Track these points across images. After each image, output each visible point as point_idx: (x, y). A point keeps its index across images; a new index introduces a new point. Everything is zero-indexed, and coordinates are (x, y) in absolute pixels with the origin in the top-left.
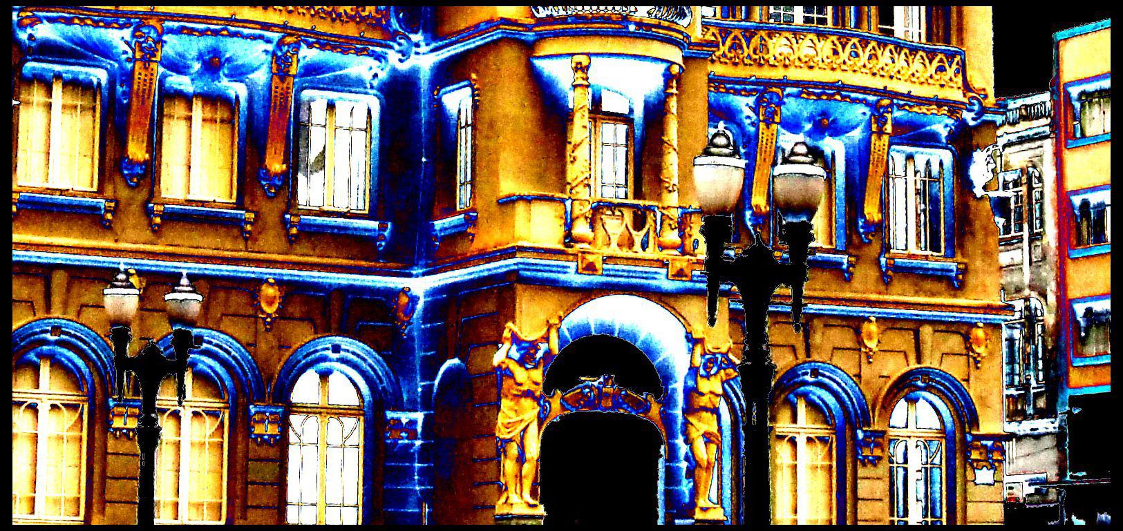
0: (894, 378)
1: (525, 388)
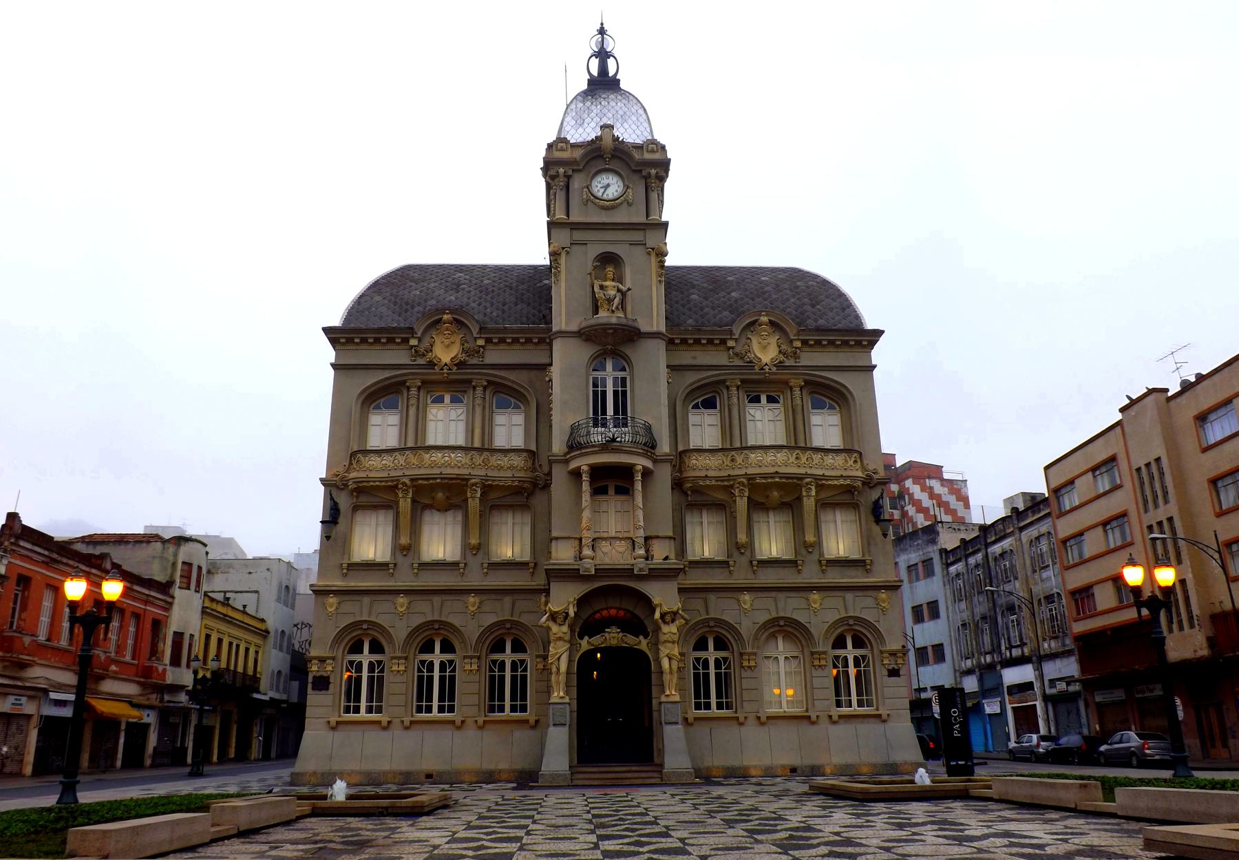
0: (831, 622)
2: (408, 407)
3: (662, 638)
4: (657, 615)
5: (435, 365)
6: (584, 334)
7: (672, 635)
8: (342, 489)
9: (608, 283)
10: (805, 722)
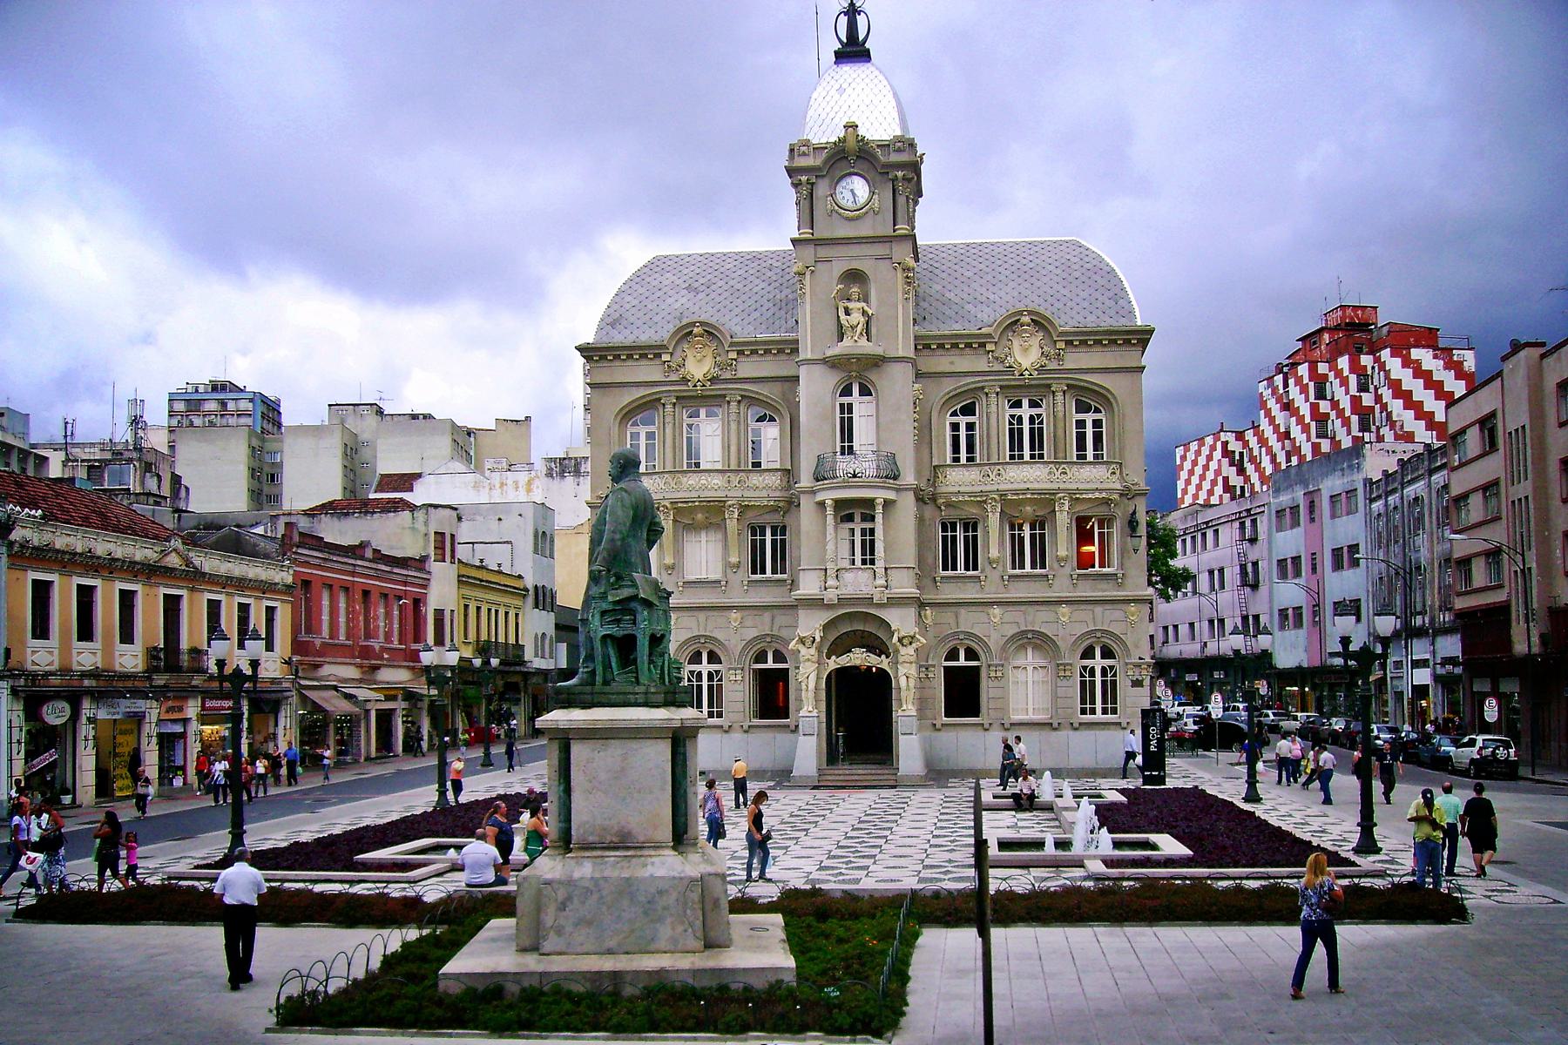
3: (901, 659)
4: (895, 639)
9: (851, 305)
10: (1047, 727)
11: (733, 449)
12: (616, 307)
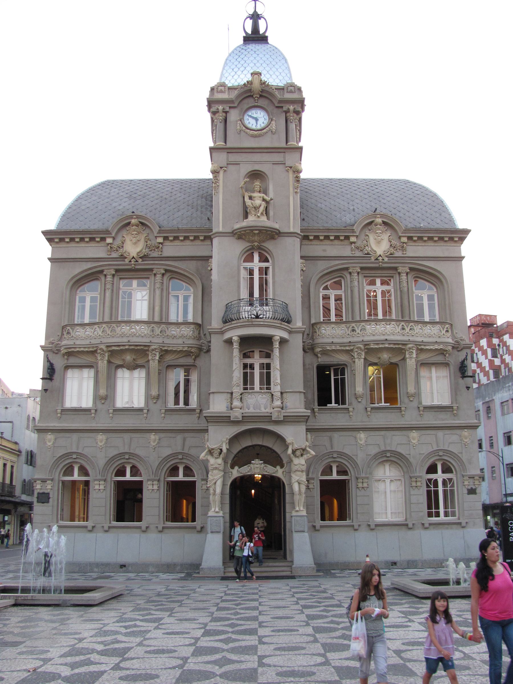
1: (214, 466)
2: (105, 290)
3: (294, 468)
4: (290, 451)
5: (126, 258)
6: (236, 234)
7: (300, 466)
8: (57, 353)
11: (157, 309)
12: (74, 208)
